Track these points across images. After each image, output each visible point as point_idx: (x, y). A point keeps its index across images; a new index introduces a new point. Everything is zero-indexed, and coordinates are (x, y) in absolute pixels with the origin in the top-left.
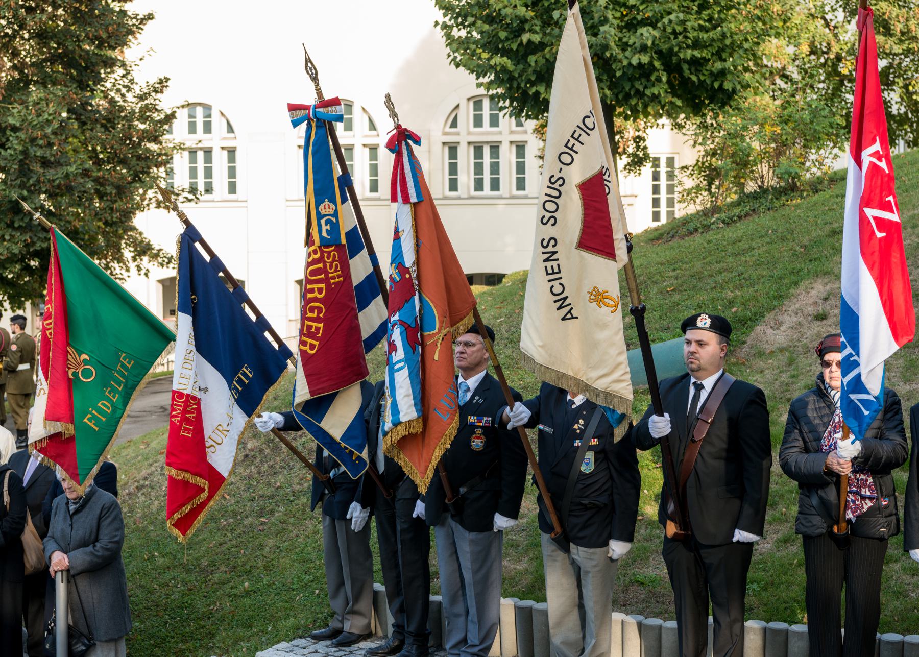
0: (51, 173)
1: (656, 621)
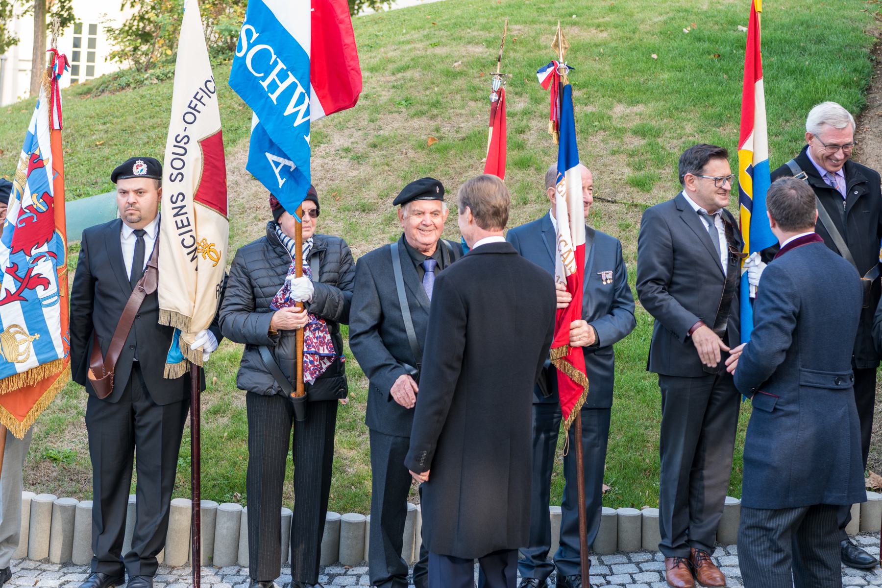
1: (71, 501)
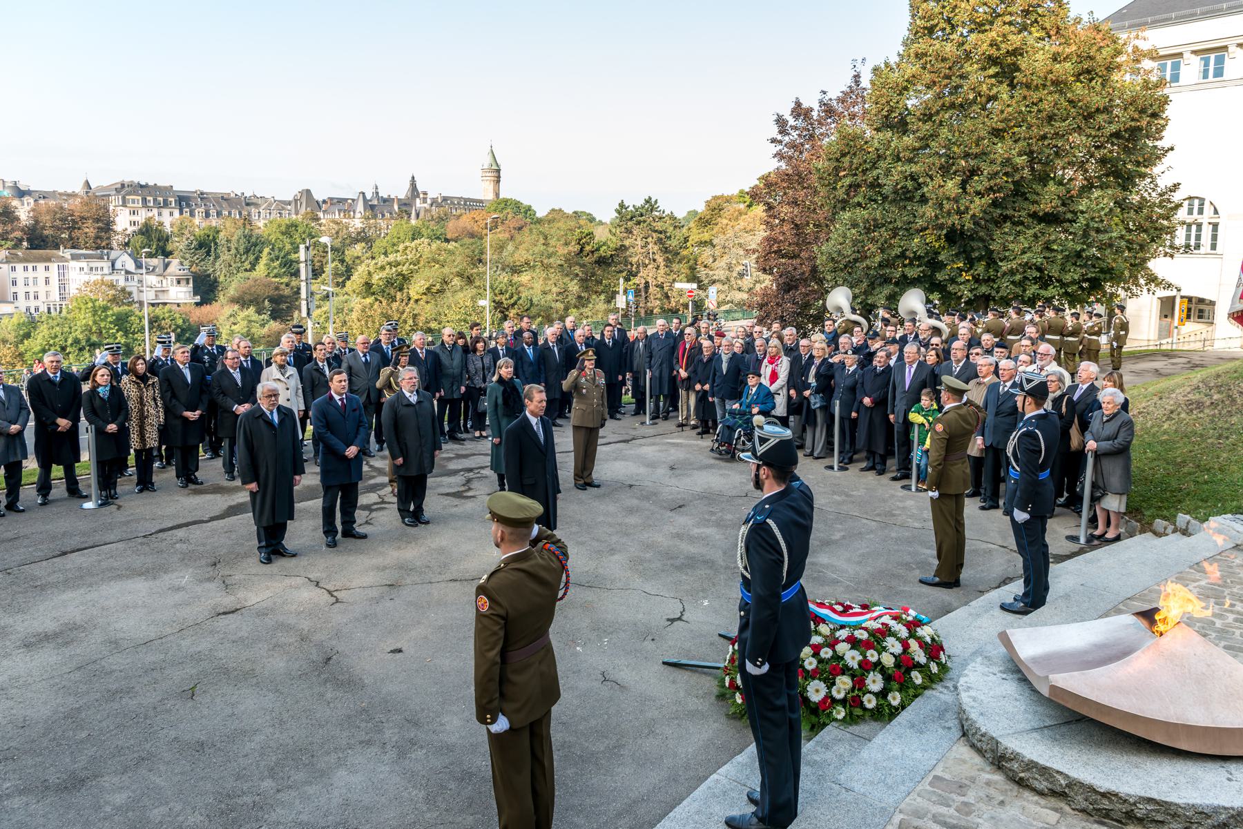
0: (1101, 237)
